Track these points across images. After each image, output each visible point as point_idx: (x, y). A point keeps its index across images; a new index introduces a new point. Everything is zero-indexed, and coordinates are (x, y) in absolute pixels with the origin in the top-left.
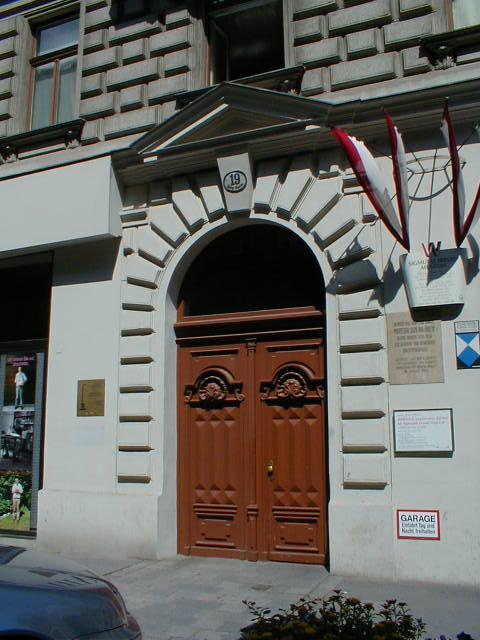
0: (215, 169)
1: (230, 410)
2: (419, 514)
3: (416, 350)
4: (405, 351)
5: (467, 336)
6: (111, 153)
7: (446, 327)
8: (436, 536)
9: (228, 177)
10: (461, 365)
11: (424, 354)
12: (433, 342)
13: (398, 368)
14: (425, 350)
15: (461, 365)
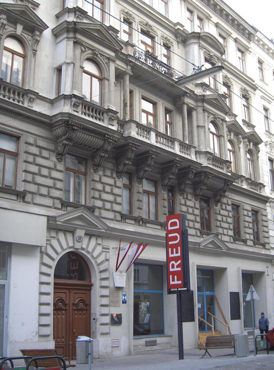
0: (73, 232)
1: (63, 312)
2: (115, 340)
3: (115, 298)
4: (113, 298)
5: (125, 295)
6: (48, 216)
7: (121, 293)
8: (118, 346)
9: (78, 237)
10: (123, 303)
11: (117, 299)
12: (118, 296)
13: (112, 302)
14: (117, 298)
15: (123, 303)
